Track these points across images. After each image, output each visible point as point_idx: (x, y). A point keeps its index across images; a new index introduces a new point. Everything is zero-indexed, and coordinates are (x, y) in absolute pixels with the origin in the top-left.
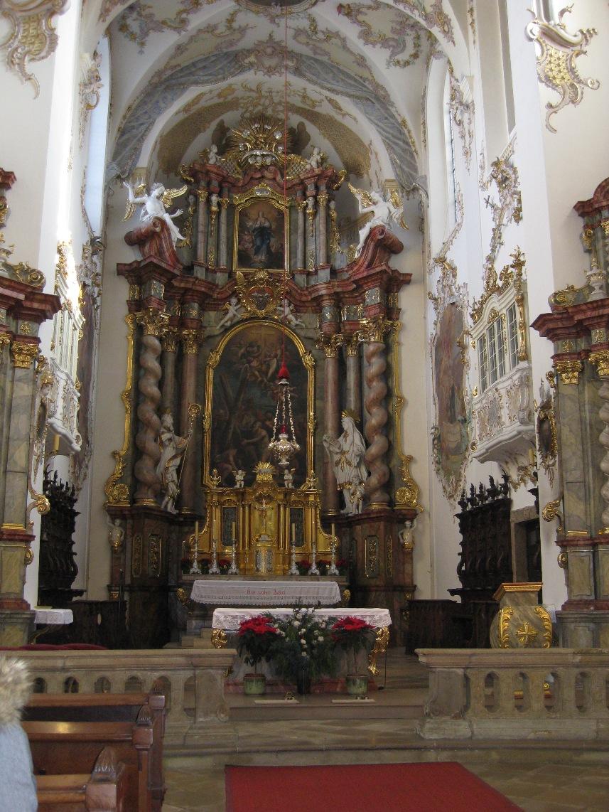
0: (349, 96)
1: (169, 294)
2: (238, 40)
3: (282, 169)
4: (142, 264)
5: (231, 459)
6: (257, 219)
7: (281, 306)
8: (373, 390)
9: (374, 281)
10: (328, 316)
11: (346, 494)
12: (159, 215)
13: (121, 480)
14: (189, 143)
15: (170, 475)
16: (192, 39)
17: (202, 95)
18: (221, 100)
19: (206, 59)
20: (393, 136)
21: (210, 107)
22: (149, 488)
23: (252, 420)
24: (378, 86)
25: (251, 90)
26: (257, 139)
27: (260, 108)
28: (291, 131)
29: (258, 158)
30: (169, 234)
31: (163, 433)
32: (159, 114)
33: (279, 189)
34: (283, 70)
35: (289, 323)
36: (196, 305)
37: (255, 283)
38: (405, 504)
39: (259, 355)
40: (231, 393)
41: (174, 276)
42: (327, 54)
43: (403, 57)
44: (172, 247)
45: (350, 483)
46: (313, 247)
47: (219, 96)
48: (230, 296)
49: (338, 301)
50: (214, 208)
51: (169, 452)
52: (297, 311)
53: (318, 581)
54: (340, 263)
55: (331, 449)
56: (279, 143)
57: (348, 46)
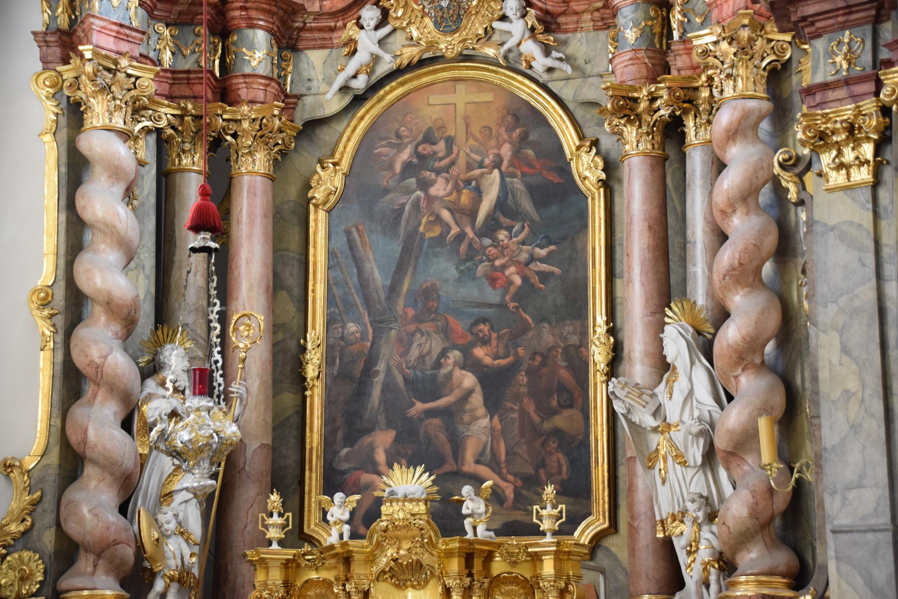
7: (504, 18)
10: (630, 35)
15: (170, 515)
22: (99, 556)
23: (436, 345)
31: (150, 397)
35: (531, 67)
36: (260, 37)
39: (453, 163)
45: (680, 516)
52: (547, 30)
55: (635, 418)
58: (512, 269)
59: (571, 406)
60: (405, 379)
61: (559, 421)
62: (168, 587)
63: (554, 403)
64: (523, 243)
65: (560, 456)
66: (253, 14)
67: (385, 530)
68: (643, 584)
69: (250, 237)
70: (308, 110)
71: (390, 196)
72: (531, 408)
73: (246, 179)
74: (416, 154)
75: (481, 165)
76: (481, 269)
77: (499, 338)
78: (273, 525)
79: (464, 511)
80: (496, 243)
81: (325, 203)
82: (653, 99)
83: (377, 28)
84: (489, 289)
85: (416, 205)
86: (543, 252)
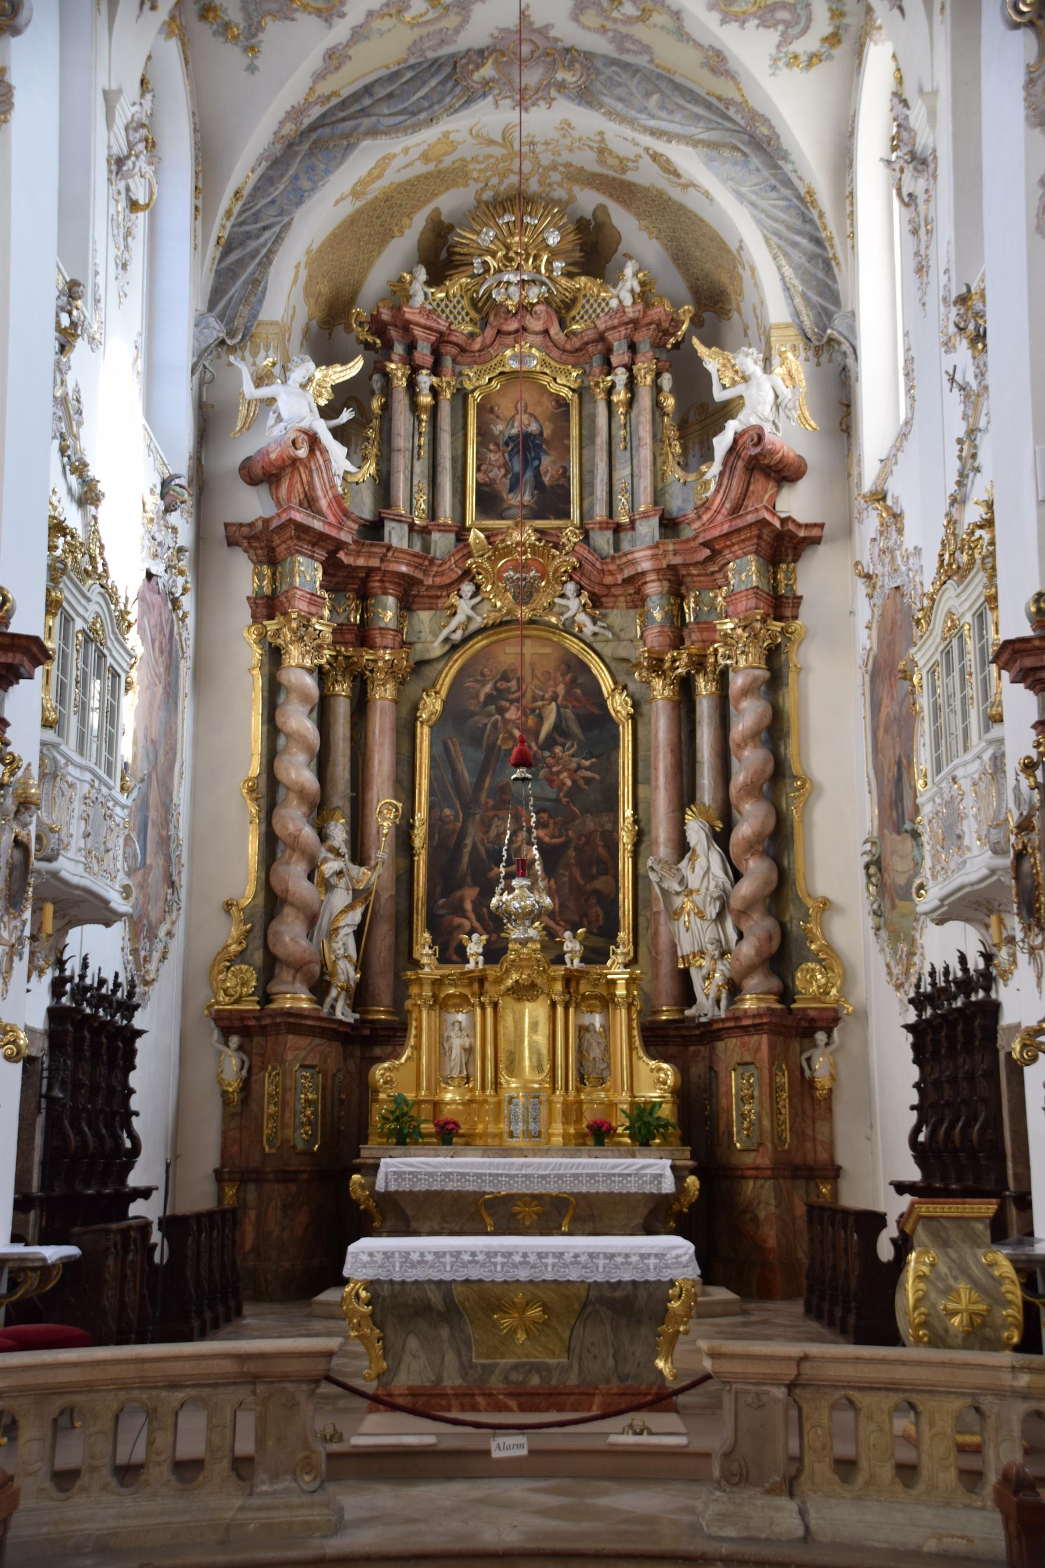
0: (695, 143)
1: (335, 580)
2: (457, 31)
3: (563, 309)
4: (275, 524)
5: (468, 906)
6: (513, 418)
7: (563, 596)
8: (748, 763)
9: (743, 541)
10: (657, 615)
11: (696, 977)
12: (305, 425)
13: (241, 957)
14: (371, 262)
15: (340, 944)
16: (358, 34)
17: (387, 159)
18: (431, 167)
19: (395, 76)
20: (789, 228)
21: (408, 182)
22: (297, 971)
24: (755, 116)
25: (491, 142)
26: (508, 248)
27: (514, 179)
28: (582, 226)
29: (512, 289)
30: (327, 461)
31: (325, 860)
32: (299, 202)
33: (556, 353)
34: (553, 93)
35: (581, 631)
36: (391, 600)
37: (508, 551)
38: (815, 999)
40: (466, 774)
41: (340, 545)
42: (646, 49)
43: (808, 44)
44: (333, 487)
45: (702, 953)
46: (627, 471)
47: (425, 157)
48: (460, 580)
49: (677, 585)
50: (426, 399)
51: (341, 898)
52: (595, 606)
53: (634, 1157)
54: (676, 504)
55: (665, 885)
56: (555, 253)
57: (688, 29)
58: (565, 774)
59: (606, 874)
60: (487, 850)
61: (599, 884)
62: (339, 994)
63: (594, 871)
64: (573, 756)
65: (598, 908)
66: (387, 585)
67: (513, 961)
68: (663, 999)
69: (382, 745)
70: (419, 652)
71: (476, 718)
72: (577, 873)
73: (378, 703)
74: (495, 687)
75: (543, 699)
76: (542, 773)
77: (555, 824)
78: (427, 955)
79: (565, 949)
80: (553, 755)
81: (429, 720)
82: (674, 660)
83: (472, 597)
84: (548, 788)
85: (495, 725)
86: (587, 763)
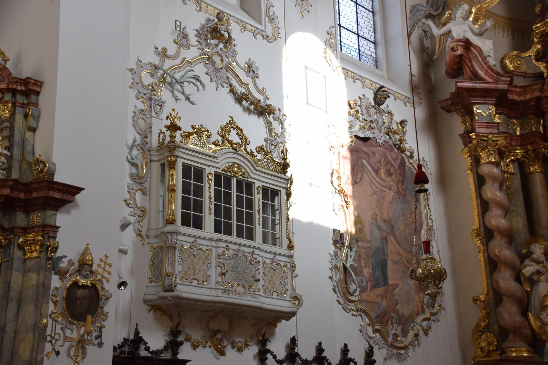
30: (480, 51)
31: (525, 266)
